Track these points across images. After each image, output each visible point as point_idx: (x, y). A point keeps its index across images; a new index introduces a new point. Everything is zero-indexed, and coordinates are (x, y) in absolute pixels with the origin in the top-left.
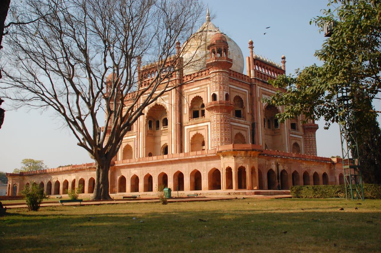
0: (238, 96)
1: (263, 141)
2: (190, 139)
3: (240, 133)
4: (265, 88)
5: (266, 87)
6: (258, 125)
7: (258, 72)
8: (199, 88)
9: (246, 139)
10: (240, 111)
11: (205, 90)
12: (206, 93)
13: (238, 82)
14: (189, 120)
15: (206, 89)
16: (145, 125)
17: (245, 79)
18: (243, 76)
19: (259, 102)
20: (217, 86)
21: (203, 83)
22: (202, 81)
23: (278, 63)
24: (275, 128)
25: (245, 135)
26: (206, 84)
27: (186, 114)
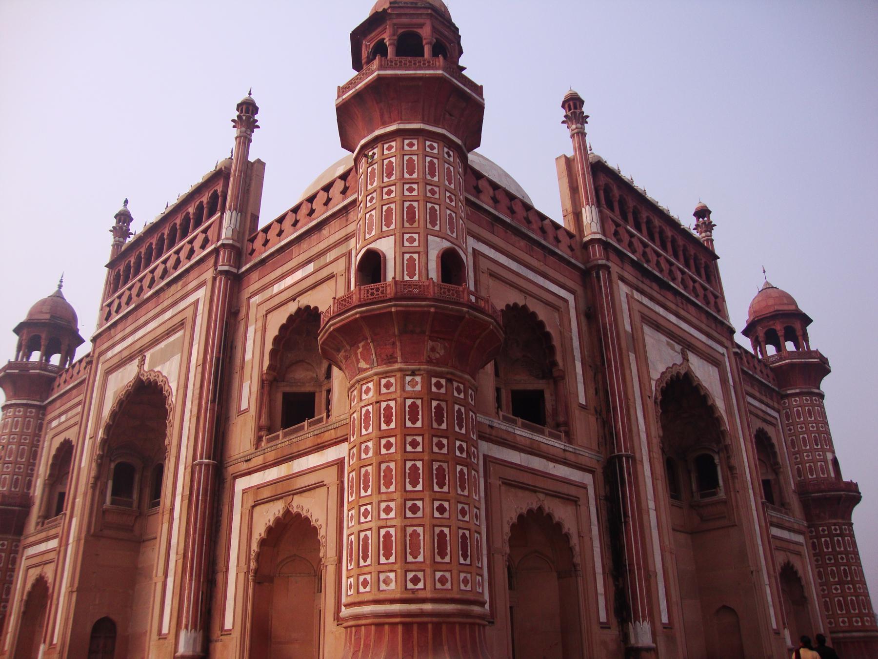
0: (524, 307)
1: (667, 554)
2: (255, 547)
3: (540, 509)
4: (652, 298)
5: (655, 294)
6: (639, 466)
7: (617, 225)
8: (310, 268)
9: (577, 548)
10: (541, 393)
11: (339, 267)
12: (341, 281)
13: (523, 243)
14: (253, 441)
15: (342, 262)
16: (91, 481)
17: (557, 240)
18: (546, 222)
19: (632, 356)
20: (389, 210)
21: (332, 234)
22: (325, 231)
23: (688, 222)
24: (702, 496)
25: (570, 526)
26: (347, 238)
27: (247, 411)
